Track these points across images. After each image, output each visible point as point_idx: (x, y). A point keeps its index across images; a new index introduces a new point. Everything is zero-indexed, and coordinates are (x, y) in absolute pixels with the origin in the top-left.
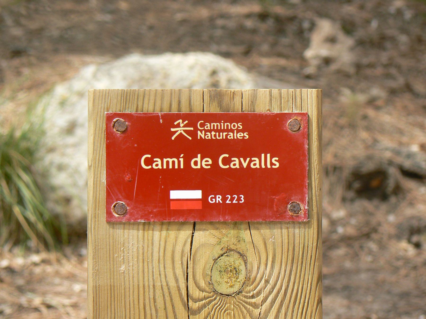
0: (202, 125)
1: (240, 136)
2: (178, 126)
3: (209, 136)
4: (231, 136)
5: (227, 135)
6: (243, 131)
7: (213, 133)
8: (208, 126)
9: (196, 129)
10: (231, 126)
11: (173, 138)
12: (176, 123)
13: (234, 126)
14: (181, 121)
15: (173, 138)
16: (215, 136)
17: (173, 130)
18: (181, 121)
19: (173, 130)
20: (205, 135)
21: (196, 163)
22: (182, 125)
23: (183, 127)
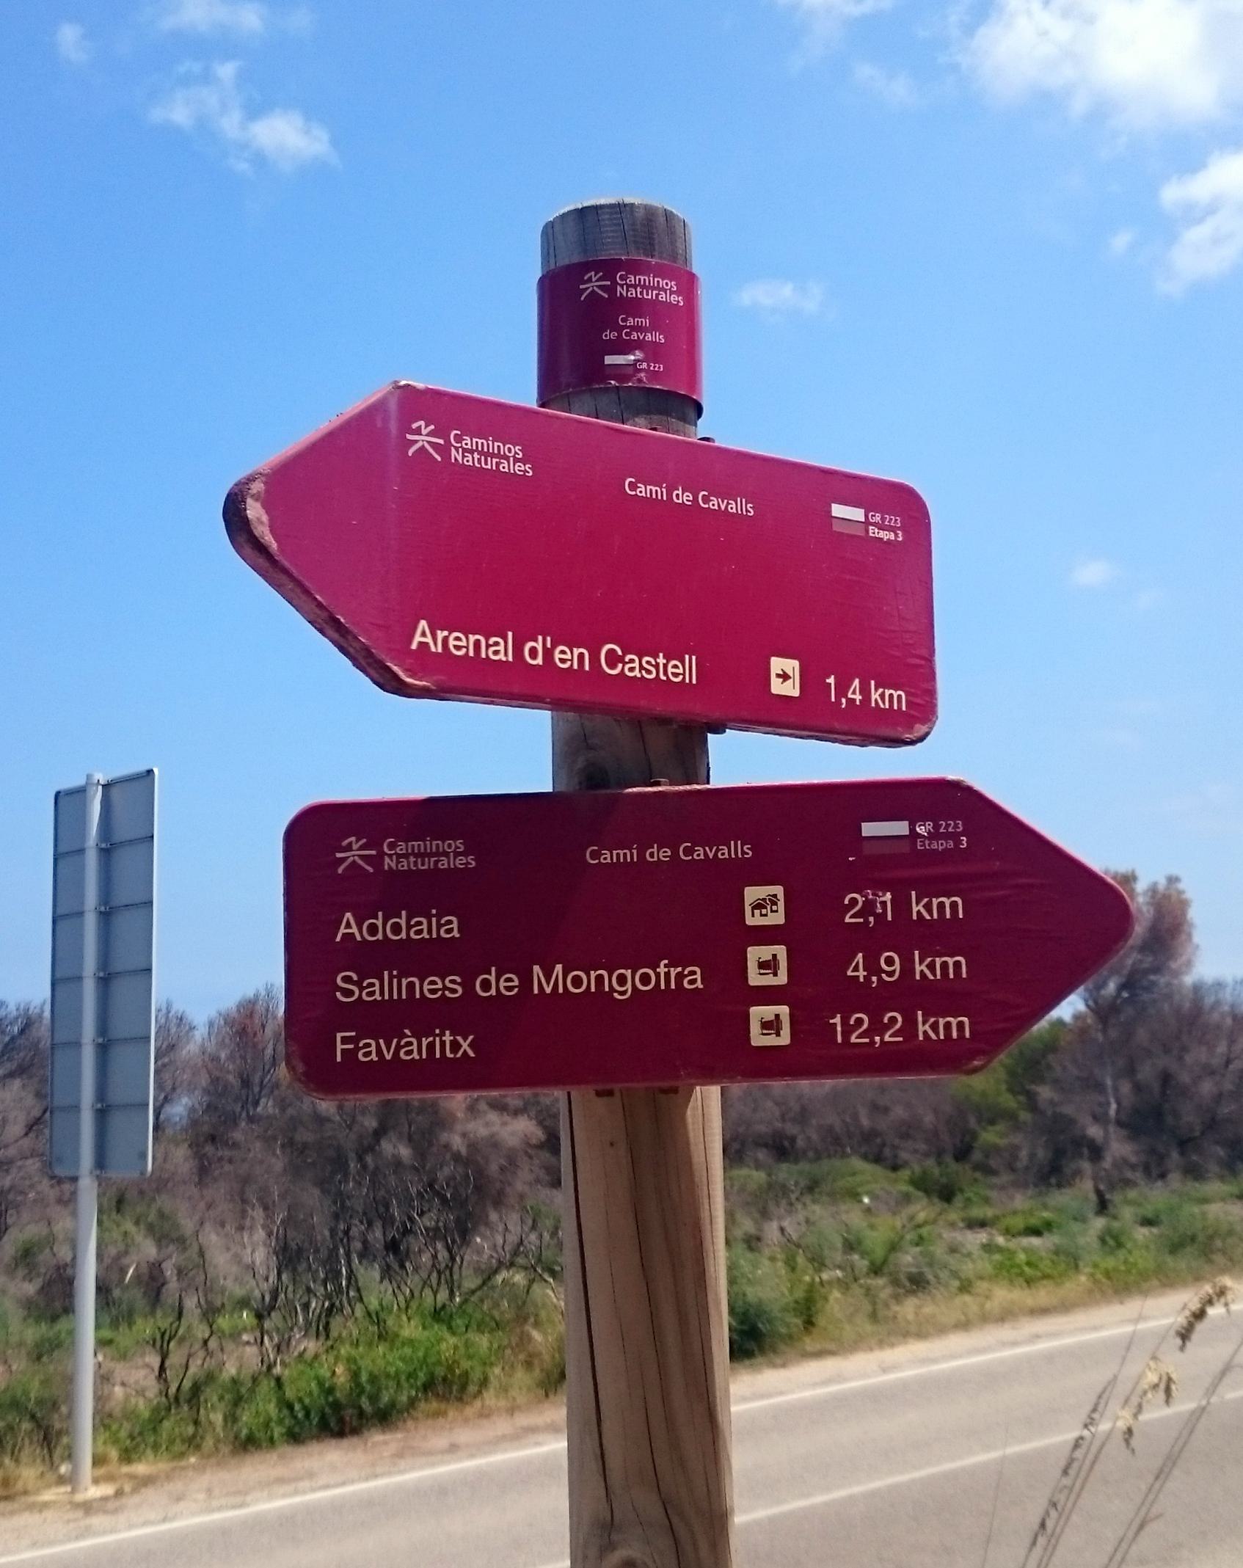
0: (392, 846)
1: (460, 862)
2: (349, 848)
4: (444, 864)
5: (436, 862)
7: (412, 859)
8: (402, 848)
12: (345, 843)
13: (450, 846)
14: (353, 839)
16: (415, 863)
17: (339, 855)
19: (339, 855)
20: (398, 862)
21: (652, 855)
22: (355, 847)
23: (361, 848)
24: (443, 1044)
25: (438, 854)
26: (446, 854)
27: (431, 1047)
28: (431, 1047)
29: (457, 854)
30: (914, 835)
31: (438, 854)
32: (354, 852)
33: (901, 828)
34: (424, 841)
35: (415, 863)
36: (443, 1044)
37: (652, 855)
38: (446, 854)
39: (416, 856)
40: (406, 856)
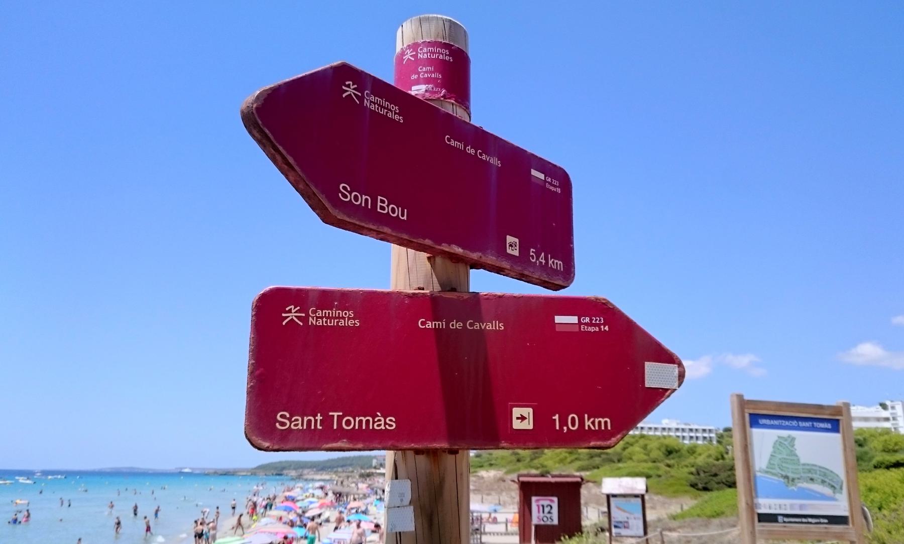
0: (314, 312)
1: (350, 323)
3: (320, 323)
4: (342, 323)
5: (338, 322)
6: (354, 319)
9: (308, 316)
10: (342, 314)
11: (284, 323)
14: (292, 307)
15: (284, 323)
16: (326, 322)
17: (284, 315)
18: (292, 307)
19: (284, 315)
24: (316, 421)
25: (339, 318)
26: (343, 318)
27: (309, 422)
28: (309, 422)
29: (349, 319)
30: (580, 323)
31: (339, 318)
32: (292, 314)
33: (574, 319)
34: (332, 310)
35: (326, 322)
36: (316, 421)
37: (453, 325)
38: (343, 318)
39: (327, 318)
40: (322, 318)
